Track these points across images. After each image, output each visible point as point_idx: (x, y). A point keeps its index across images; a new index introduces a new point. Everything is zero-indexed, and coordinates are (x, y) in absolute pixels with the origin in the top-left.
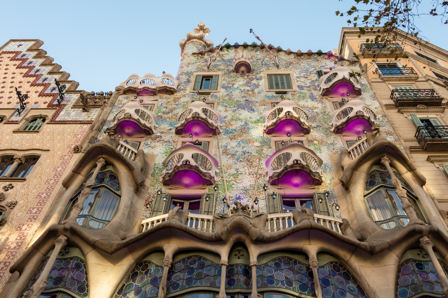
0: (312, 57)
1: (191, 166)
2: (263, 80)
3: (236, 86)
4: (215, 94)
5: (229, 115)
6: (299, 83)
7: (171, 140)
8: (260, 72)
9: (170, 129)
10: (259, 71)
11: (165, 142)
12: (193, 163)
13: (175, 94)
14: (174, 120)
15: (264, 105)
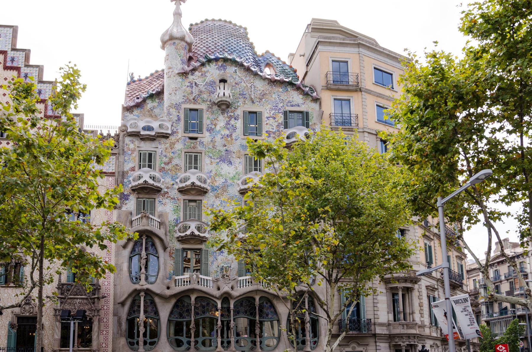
0: (283, 85)
1: (195, 236)
2: (240, 120)
3: (218, 128)
4: (203, 140)
5: (213, 167)
6: (268, 126)
7: (175, 197)
8: (238, 106)
9: (173, 185)
10: (236, 105)
11: (172, 199)
12: (197, 233)
13: (171, 137)
14: (174, 173)
15: (239, 157)
